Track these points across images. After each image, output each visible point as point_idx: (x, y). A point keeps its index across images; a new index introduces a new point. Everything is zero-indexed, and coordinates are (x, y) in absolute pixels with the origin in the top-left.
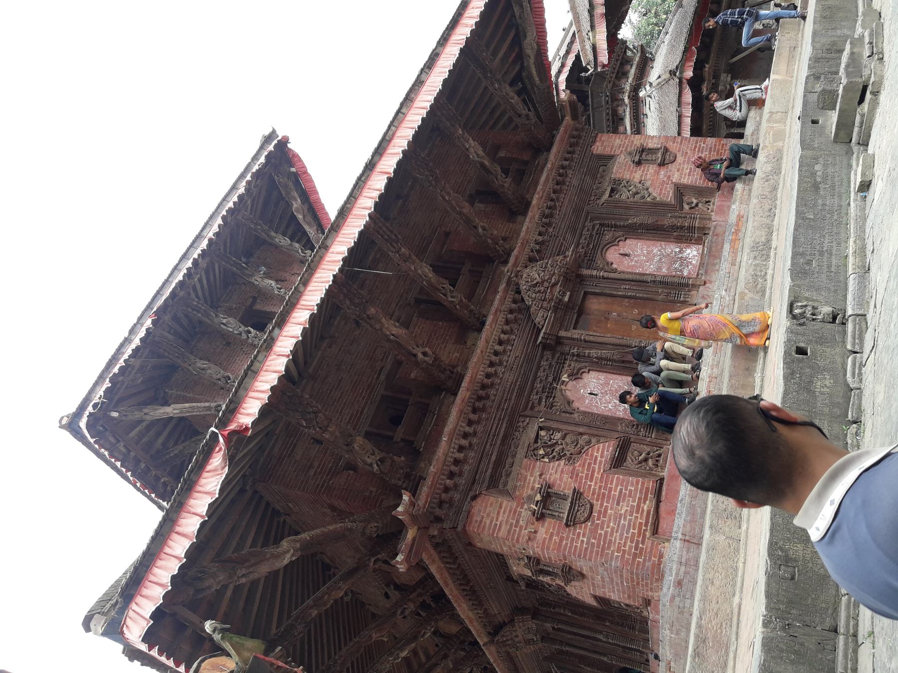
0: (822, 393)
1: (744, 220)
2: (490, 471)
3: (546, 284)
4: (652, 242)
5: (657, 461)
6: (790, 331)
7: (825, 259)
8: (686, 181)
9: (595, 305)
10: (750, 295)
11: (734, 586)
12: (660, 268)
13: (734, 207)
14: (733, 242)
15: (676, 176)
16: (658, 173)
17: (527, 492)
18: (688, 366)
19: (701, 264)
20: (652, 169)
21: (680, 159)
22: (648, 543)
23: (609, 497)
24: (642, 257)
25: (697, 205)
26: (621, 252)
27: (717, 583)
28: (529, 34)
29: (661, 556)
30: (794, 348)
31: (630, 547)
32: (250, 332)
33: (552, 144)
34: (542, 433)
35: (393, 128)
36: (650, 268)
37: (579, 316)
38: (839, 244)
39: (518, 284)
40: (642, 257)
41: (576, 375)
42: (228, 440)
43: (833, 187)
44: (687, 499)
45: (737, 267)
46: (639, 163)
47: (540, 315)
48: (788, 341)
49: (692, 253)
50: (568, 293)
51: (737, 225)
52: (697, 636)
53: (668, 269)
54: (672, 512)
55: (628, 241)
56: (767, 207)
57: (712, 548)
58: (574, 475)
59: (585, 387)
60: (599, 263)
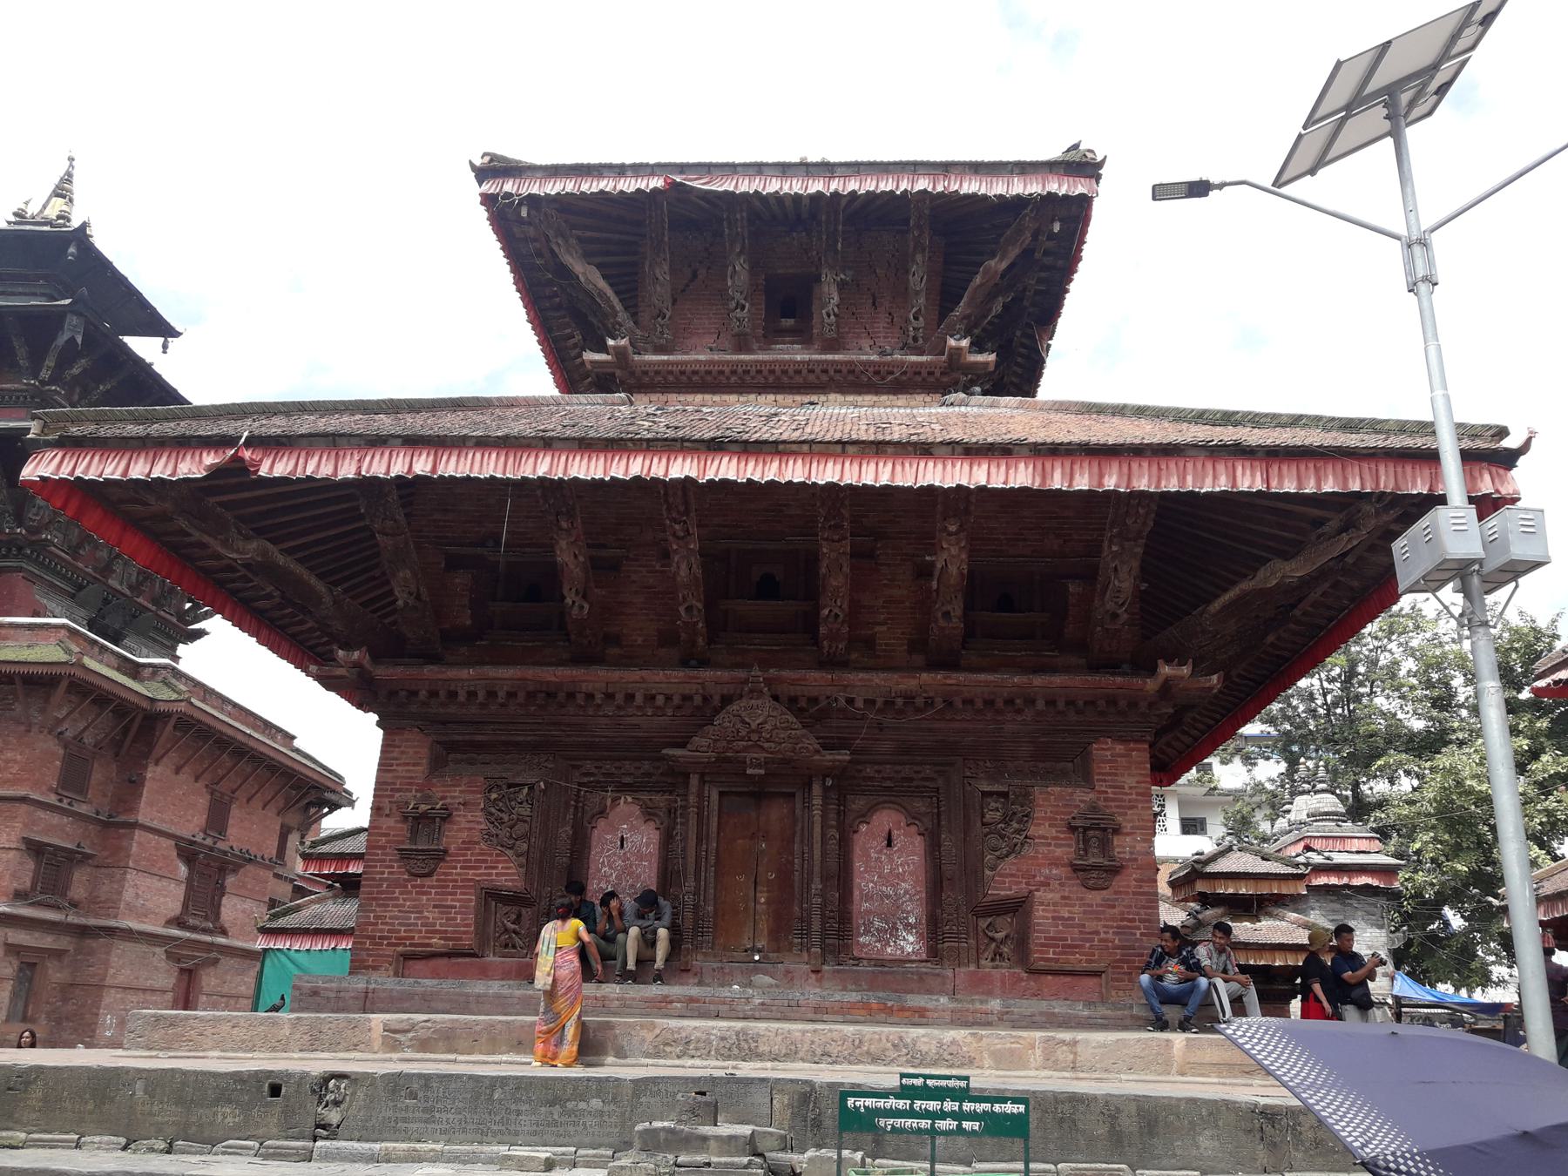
0: (215, 1114)
1: (916, 1019)
2: (460, 738)
3: (754, 737)
4: (922, 877)
5: (506, 946)
6: (304, 1076)
7: (417, 1115)
8: (1041, 915)
9: (775, 814)
10: (650, 1037)
11: (233, 1050)
12: (868, 898)
13: (943, 1000)
14: (866, 1006)
15: (1050, 896)
16: (1055, 863)
17: (437, 792)
18: (631, 965)
19: (881, 963)
20: (1065, 850)
21: (1095, 898)
22: (390, 951)
23: (443, 894)
24: (889, 868)
25: (993, 939)
26: (895, 833)
27: (235, 1031)
28: (1293, 564)
29: (375, 968)
30: (278, 1081)
31: (382, 931)
32: (743, 308)
33: (1094, 668)
34: (526, 790)
35: (805, 448)
36: (865, 882)
37: (752, 794)
38: (444, 1132)
39: (741, 697)
40: (889, 868)
41: (649, 814)
42: (236, 458)
43: (555, 1123)
44: (419, 989)
45: (811, 1016)
46: (1072, 829)
47: (704, 742)
48: (288, 1075)
49: (909, 943)
50: (762, 772)
51: (902, 1009)
52: (176, 1016)
53: (868, 912)
54: (435, 974)
55: (918, 840)
56: (834, 1049)
57: (275, 1023)
58: (468, 844)
59: (632, 828)
60: (858, 803)
